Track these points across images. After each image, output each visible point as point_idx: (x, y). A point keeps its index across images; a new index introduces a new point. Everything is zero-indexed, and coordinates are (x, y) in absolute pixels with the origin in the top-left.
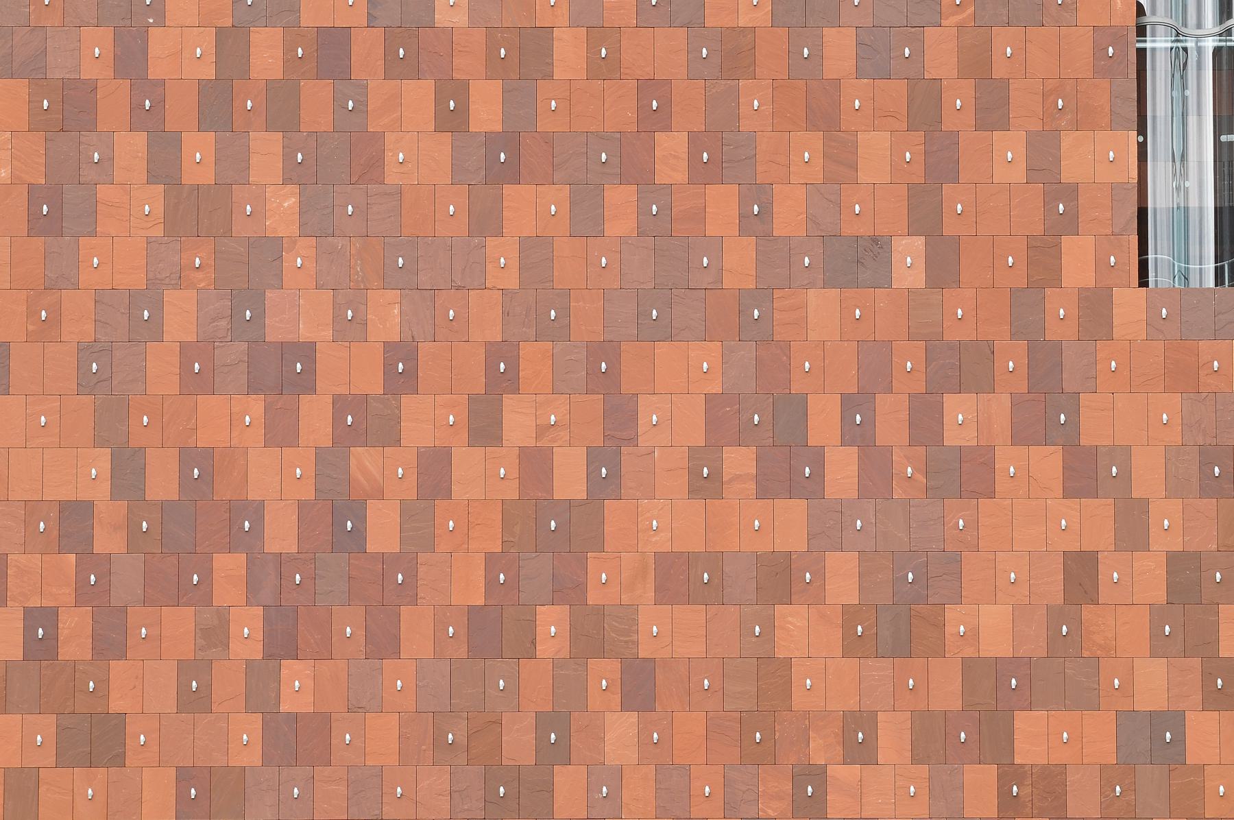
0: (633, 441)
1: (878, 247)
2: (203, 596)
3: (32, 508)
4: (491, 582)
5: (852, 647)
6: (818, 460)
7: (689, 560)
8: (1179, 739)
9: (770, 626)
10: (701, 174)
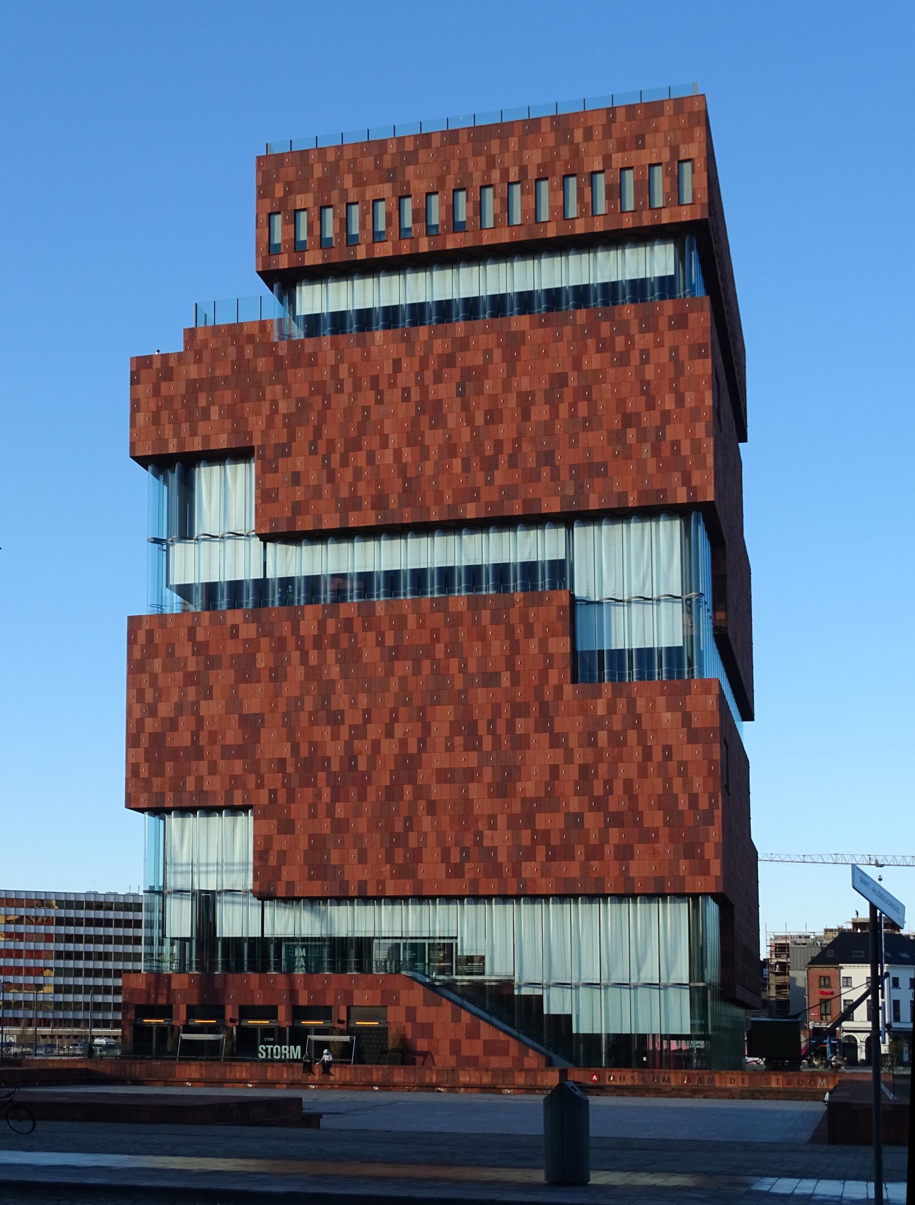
0: (430, 735)
1: (497, 674)
2: (314, 785)
3: (270, 761)
4: (391, 778)
5: (490, 796)
6: (480, 739)
7: (445, 770)
8: (582, 820)
9: (467, 791)
10: (448, 656)
